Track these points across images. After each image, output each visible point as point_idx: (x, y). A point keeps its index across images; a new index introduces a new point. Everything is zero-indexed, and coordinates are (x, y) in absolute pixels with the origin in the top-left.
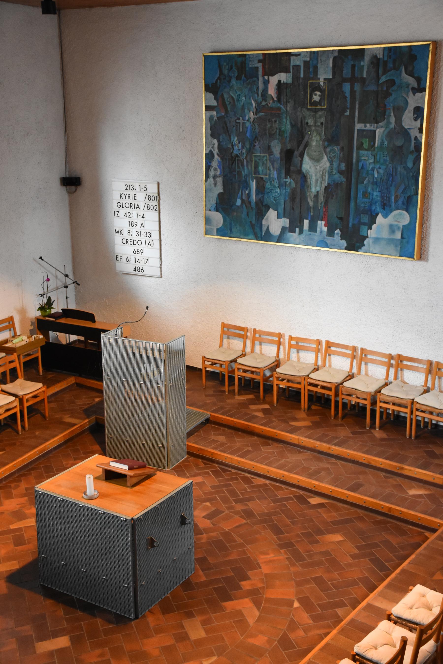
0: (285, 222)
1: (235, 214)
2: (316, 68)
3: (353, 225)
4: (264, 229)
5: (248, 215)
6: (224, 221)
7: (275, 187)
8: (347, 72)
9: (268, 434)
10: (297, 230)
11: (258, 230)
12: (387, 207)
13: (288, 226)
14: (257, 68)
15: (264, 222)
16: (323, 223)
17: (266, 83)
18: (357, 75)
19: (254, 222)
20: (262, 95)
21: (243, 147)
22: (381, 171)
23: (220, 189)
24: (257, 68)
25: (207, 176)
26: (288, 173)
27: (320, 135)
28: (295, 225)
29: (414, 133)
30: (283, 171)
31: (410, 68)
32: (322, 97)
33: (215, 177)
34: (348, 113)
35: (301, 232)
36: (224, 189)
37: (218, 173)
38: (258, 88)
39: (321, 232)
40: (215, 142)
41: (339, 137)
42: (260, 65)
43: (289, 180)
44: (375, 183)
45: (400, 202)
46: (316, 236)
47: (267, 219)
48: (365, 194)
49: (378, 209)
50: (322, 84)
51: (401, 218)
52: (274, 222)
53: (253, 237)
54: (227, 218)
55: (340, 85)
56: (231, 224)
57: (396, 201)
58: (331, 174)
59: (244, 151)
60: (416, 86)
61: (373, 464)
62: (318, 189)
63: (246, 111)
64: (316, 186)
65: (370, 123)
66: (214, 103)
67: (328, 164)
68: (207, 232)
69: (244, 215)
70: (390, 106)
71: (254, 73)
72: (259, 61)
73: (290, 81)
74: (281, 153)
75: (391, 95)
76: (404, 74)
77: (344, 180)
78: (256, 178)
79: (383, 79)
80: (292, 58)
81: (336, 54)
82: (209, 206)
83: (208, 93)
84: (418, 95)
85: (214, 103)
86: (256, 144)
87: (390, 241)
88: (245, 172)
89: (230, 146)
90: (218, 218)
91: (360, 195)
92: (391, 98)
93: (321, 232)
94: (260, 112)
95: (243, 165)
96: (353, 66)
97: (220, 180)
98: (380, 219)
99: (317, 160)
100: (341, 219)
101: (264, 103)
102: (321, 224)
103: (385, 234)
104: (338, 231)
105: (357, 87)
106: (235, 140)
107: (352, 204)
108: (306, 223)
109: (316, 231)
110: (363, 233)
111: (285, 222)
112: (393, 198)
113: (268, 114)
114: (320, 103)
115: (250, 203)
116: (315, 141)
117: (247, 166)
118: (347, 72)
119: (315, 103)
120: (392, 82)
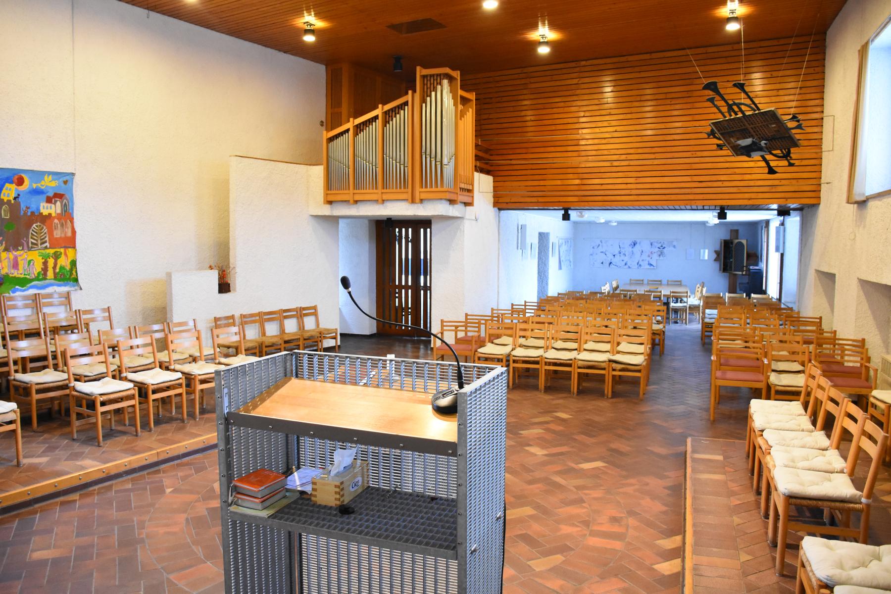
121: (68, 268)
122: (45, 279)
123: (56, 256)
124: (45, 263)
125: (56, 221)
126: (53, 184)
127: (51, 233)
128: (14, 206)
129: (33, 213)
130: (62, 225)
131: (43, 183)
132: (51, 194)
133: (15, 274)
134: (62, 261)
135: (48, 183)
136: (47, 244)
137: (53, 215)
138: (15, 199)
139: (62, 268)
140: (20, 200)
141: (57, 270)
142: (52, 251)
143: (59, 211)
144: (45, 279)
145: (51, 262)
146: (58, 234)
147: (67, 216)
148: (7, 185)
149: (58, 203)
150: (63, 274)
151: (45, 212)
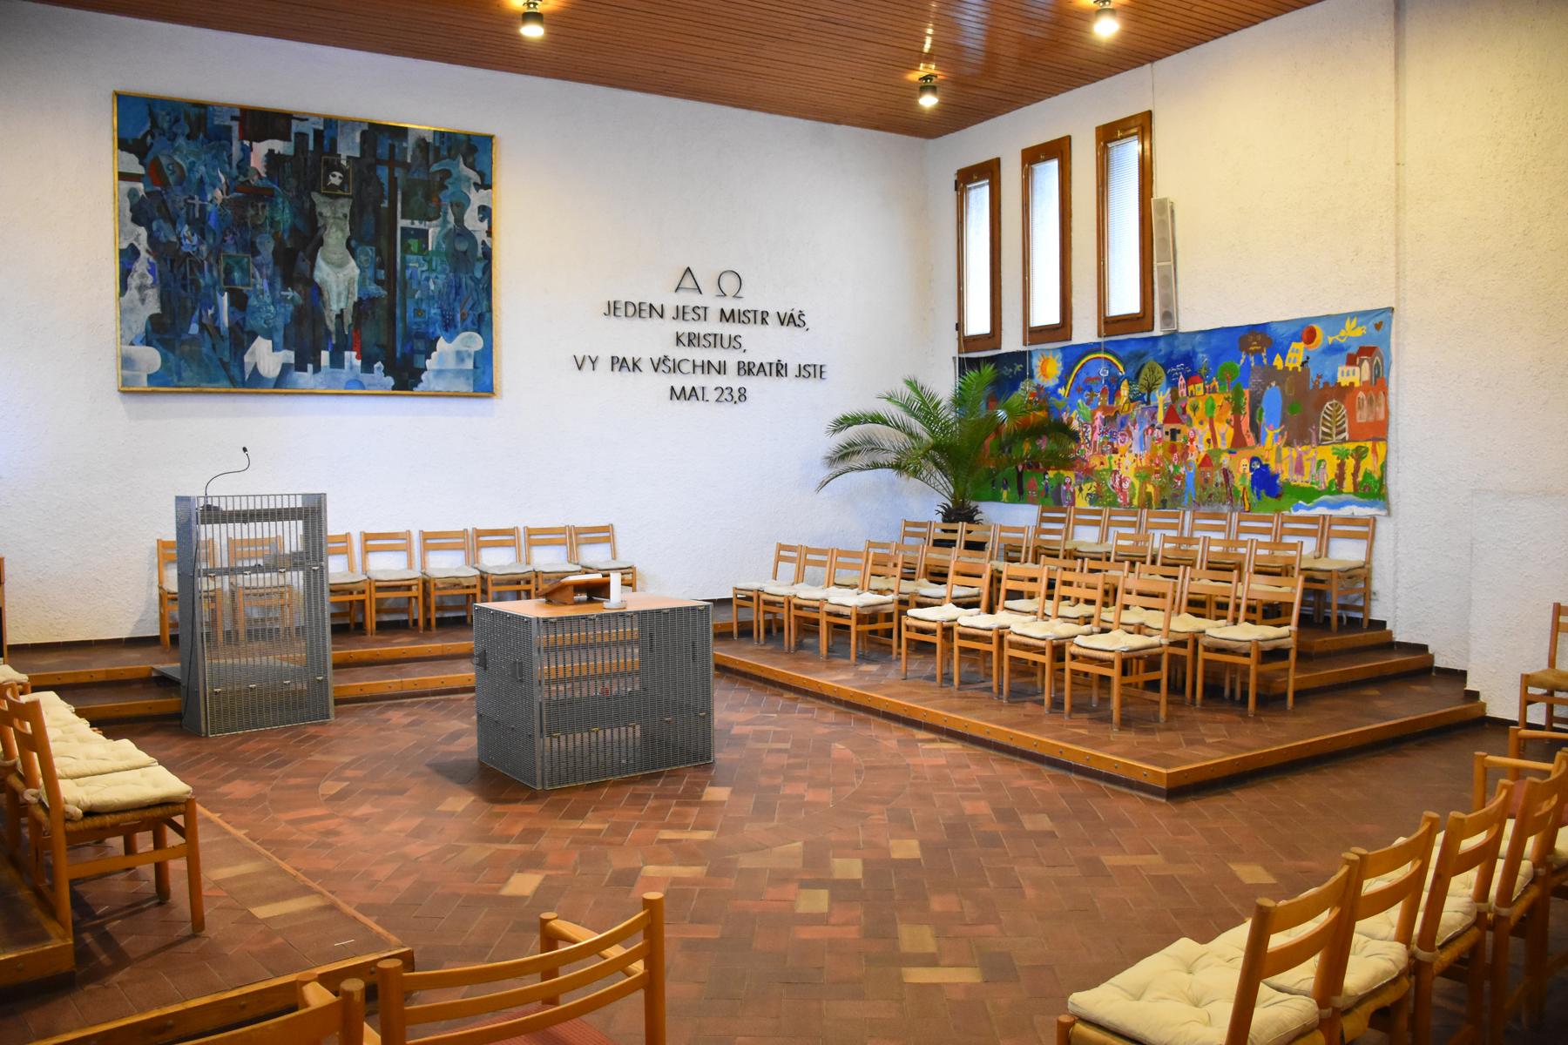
0: (289, 356)
1: (186, 348)
3: (403, 355)
4: (248, 370)
5: (214, 347)
6: (164, 360)
7: (266, 304)
8: (383, 151)
9: (387, 657)
10: (310, 367)
11: (235, 372)
13: (293, 361)
15: (247, 358)
16: (354, 354)
17: (247, 152)
18: (398, 157)
19: (226, 359)
20: (238, 167)
21: (200, 243)
22: (439, 282)
23: (153, 307)
24: (229, 128)
25: (124, 286)
26: (288, 282)
27: (343, 230)
28: (306, 359)
29: (481, 236)
31: (470, 160)
32: (345, 179)
33: (141, 288)
34: (385, 204)
35: (317, 369)
36: (163, 307)
37: (150, 280)
39: (352, 367)
41: (373, 235)
42: (235, 125)
43: (290, 293)
44: (430, 298)
46: (344, 374)
47: (253, 353)
48: (418, 312)
49: (438, 332)
50: (344, 162)
52: (266, 357)
53: (226, 383)
54: (171, 356)
55: (372, 168)
56: (179, 366)
57: (463, 320)
58: (362, 283)
59: (204, 248)
60: (479, 181)
62: (342, 305)
63: (207, 188)
64: (339, 301)
65: (421, 220)
66: (141, 170)
67: (357, 271)
68: (125, 382)
69: (206, 349)
70: (446, 202)
71: (223, 134)
72: (233, 118)
74: (275, 253)
76: (462, 166)
77: (384, 293)
78: (229, 291)
79: (435, 168)
80: (294, 123)
81: (366, 127)
82: (130, 337)
83: (125, 154)
84: (482, 191)
85: (141, 170)
86: (228, 238)
87: (459, 373)
89: (174, 239)
90: (151, 358)
91: (410, 313)
93: (352, 367)
94: (236, 190)
95: (201, 270)
96: (392, 147)
97: (153, 295)
98: (442, 344)
99: (341, 265)
101: (242, 179)
102: (351, 357)
103: (451, 364)
104: (379, 364)
106: (186, 230)
107: (399, 325)
108: (325, 356)
109: (342, 366)
110: (419, 365)
111: (289, 356)
113: (249, 195)
114: (341, 187)
115: (218, 329)
116: (335, 238)
117: (210, 271)
118: (383, 151)
120: (447, 174)
121: (1376, 477)
122: (1339, 492)
123: (1359, 455)
124: (1341, 466)
125: (1361, 394)
126: (1359, 332)
127: (1352, 414)
128: (1299, 378)
129: (1326, 384)
130: (1370, 402)
131: (1342, 333)
132: (1353, 350)
133: (1300, 481)
134: (1368, 464)
135: (1353, 332)
136: (1346, 434)
137: (1357, 384)
138: (1303, 364)
139: (1368, 474)
140: (1309, 365)
141: (1360, 479)
142: (1351, 446)
143: (1366, 377)
144: (1339, 492)
145: (1350, 463)
146: (1363, 416)
147: (1378, 383)
148: (1294, 345)
149: (1366, 365)
150: (1368, 487)
151: (1344, 381)
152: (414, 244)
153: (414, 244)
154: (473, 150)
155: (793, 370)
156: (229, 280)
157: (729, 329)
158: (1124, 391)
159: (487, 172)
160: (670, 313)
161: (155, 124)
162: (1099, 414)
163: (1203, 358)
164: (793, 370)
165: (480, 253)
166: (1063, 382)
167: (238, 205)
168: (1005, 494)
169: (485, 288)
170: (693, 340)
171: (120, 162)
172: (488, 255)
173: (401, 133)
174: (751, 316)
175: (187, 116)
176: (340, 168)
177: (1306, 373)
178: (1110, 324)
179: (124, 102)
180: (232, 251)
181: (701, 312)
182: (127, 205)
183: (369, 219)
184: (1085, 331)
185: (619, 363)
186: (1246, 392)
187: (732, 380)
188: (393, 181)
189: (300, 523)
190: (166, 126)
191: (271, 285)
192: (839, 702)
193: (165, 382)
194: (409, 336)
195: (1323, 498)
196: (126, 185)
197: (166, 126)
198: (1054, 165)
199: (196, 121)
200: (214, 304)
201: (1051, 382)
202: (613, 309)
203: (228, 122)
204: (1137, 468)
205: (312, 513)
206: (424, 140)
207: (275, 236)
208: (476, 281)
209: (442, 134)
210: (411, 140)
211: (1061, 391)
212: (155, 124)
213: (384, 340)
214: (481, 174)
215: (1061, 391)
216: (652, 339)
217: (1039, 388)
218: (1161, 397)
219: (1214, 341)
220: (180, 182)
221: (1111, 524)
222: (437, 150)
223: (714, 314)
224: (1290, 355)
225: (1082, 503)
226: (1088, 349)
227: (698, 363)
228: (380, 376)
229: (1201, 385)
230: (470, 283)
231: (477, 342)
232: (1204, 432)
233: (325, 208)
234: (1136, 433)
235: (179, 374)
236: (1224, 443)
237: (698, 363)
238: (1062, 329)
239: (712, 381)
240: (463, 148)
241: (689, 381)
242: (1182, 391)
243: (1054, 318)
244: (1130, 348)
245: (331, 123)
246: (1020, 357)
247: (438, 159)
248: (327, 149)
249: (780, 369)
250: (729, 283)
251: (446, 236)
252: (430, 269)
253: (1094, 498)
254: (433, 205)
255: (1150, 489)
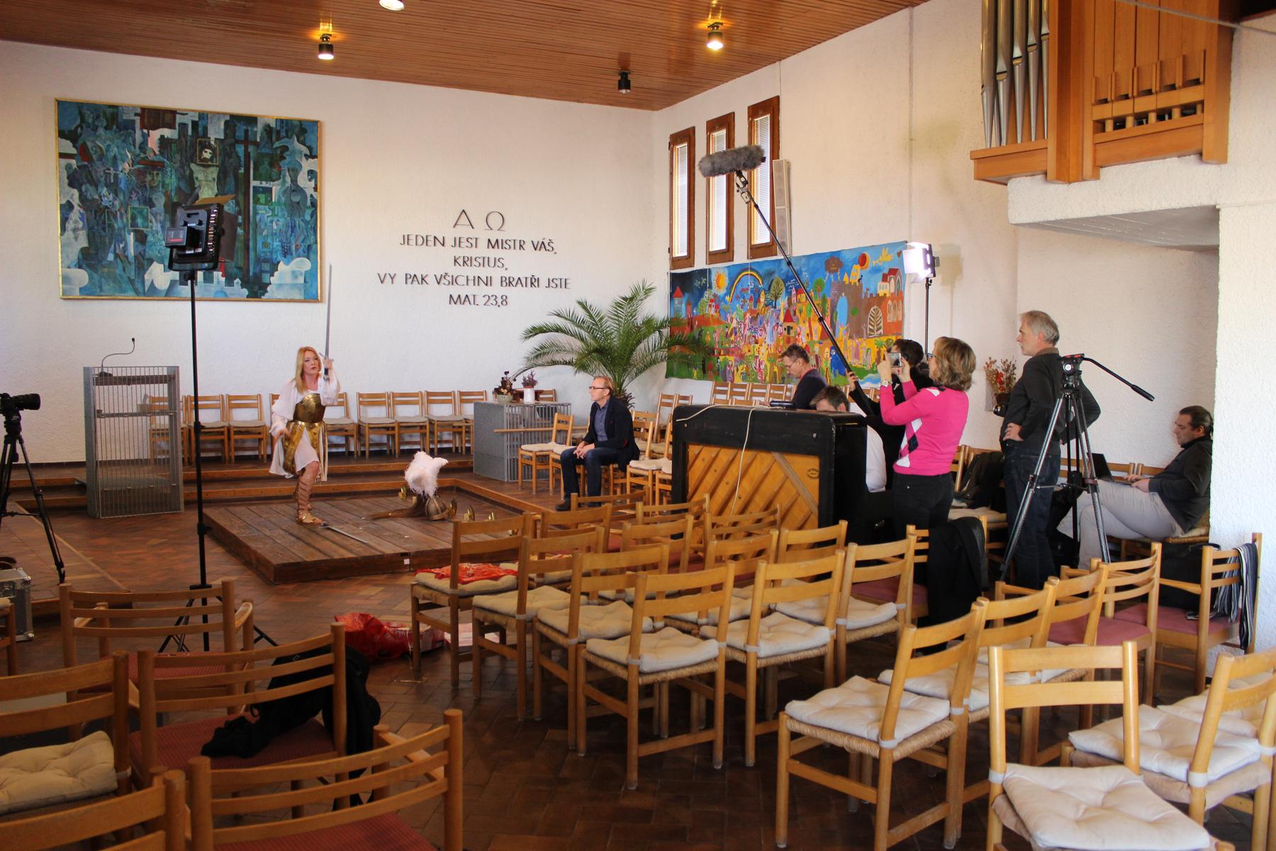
0: (176, 275)
2: (205, 129)
4: (147, 284)
6: (91, 278)
8: (240, 134)
11: (139, 286)
12: (286, 253)
14: (134, 121)
15: (146, 277)
17: (145, 137)
23: (83, 242)
24: (134, 121)
25: (63, 229)
29: (310, 191)
30: (168, 224)
33: (75, 230)
34: (242, 171)
36: (89, 243)
37: (81, 225)
38: (134, 141)
40: (76, 192)
42: (138, 119)
44: (273, 234)
45: (301, 251)
46: (213, 287)
48: (265, 244)
51: (302, 264)
52: (160, 275)
53: (131, 294)
55: (233, 146)
57: (297, 250)
59: (117, 203)
61: (352, 471)
63: (119, 162)
65: (267, 181)
66: (74, 151)
69: (119, 271)
71: (129, 126)
73: (176, 137)
75: (284, 158)
79: (277, 144)
82: (67, 263)
85: (74, 151)
86: (133, 196)
87: (294, 286)
88: (118, 224)
89: (97, 197)
90: (82, 276)
91: (259, 245)
92: (286, 161)
95: (115, 217)
96: (246, 132)
97: (83, 235)
98: (281, 266)
100: (240, 268)
103: (288, 280)
105: (251, 149)
106: (104, 191)
107: (252, 254)
108: (200, 275)
112: (293, 247)
113: (150, 166)
114: (211, 160)
115: (127, 257)
118: (240, 134)
119: (205, 160)
120: (285, 148)
127: (885, 316)
132: (886, 271)
135: (886, 261)
142: (884, 339)
146: (891, 318)
152: (262, 197)
153: (262, 197)
154: (305, 131)
155: (544, 282)
156: (134, 224)
157: (497, 253)
158: (762, 300)
159: (314, 145)
160: (450, 242)
161: (83, 120)
162: (748, 315)
163: (805, 276)
164: (544, 282)
165: (309, 203)
166: (728, 293)
167: (140, 174)
168: (695, 372)
169: (313, 227)
170: (467, 261)
171: (59, 145)
172: (314, 205)
173: (252, 120)
174: (511, 244)
175: (105, 114)
176: (210, 147)
177: (861, 286)
178: (755, 251)
179: (62, 105)
180: (136, 205)
181: (473, 242)
182: (65, 174)
183: (231, 182)
184: (741, 256)
185: (411, 278)
186: (829, 299)
187: (497, 290)
188: (247, 155)
189: (166, 385)
190: (90, 121)
191: (163, 227)
192: (509, 508)
193: (89, 292)
194: (259, 261)
195: (870, 375)
196: (64, 162)
197: (90, 121)
198: (723, 132)
199: (112, 118)
200: (124, 240)
201: (721, 292)
202: (406, 240)
203: (133, 118)
204: (769, 355)
205: (171, 379)
206: (268, 126)
207: (166, 194)
208: (307, 223)
209: (282, 121)
210: (259, 128)
211: (728, 298)
212: (83, 120)
213: (241, 263)
214: (310, 148)
215: (728, 298)
216: (437, 261)
217: (715, 296)
218: (782, 303)
219: (812, 263)
220: (100, 159)
221: (753, 394)
222: (278, 132)
223: (483, 243)
224: (853, 273)
225: (738, 380)
226: (743, 268)
227: (471, 278)
228: (238, 288)
229: (804, 295)
230: (302, 224)
231: (306, 265)
232: (804, 328)
233: (199, 173)
234: (769, 328)
235: (100, 287)
236: (816, 337)
237: (471, 278)
238: (727, 254)
239: (482, 290)
240: (297, 130)
241: (462, 291)
242: (794, 299)
243: (723, 246)
244: (767, 268)
245: (203, 115)
246: (703, 273)
247: (278, 139)
248: (201, 133)
249: (534, 282)
250: (495, 221)
251: (285, 192)
252: (274, 215)
253: (746, 376)
254: (275, 170)
255: (776, 369)
